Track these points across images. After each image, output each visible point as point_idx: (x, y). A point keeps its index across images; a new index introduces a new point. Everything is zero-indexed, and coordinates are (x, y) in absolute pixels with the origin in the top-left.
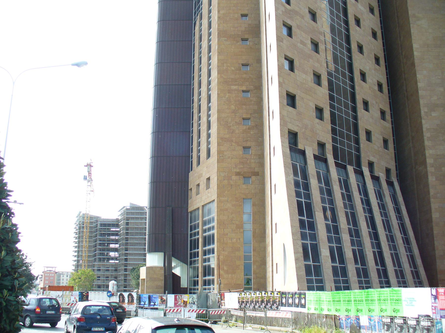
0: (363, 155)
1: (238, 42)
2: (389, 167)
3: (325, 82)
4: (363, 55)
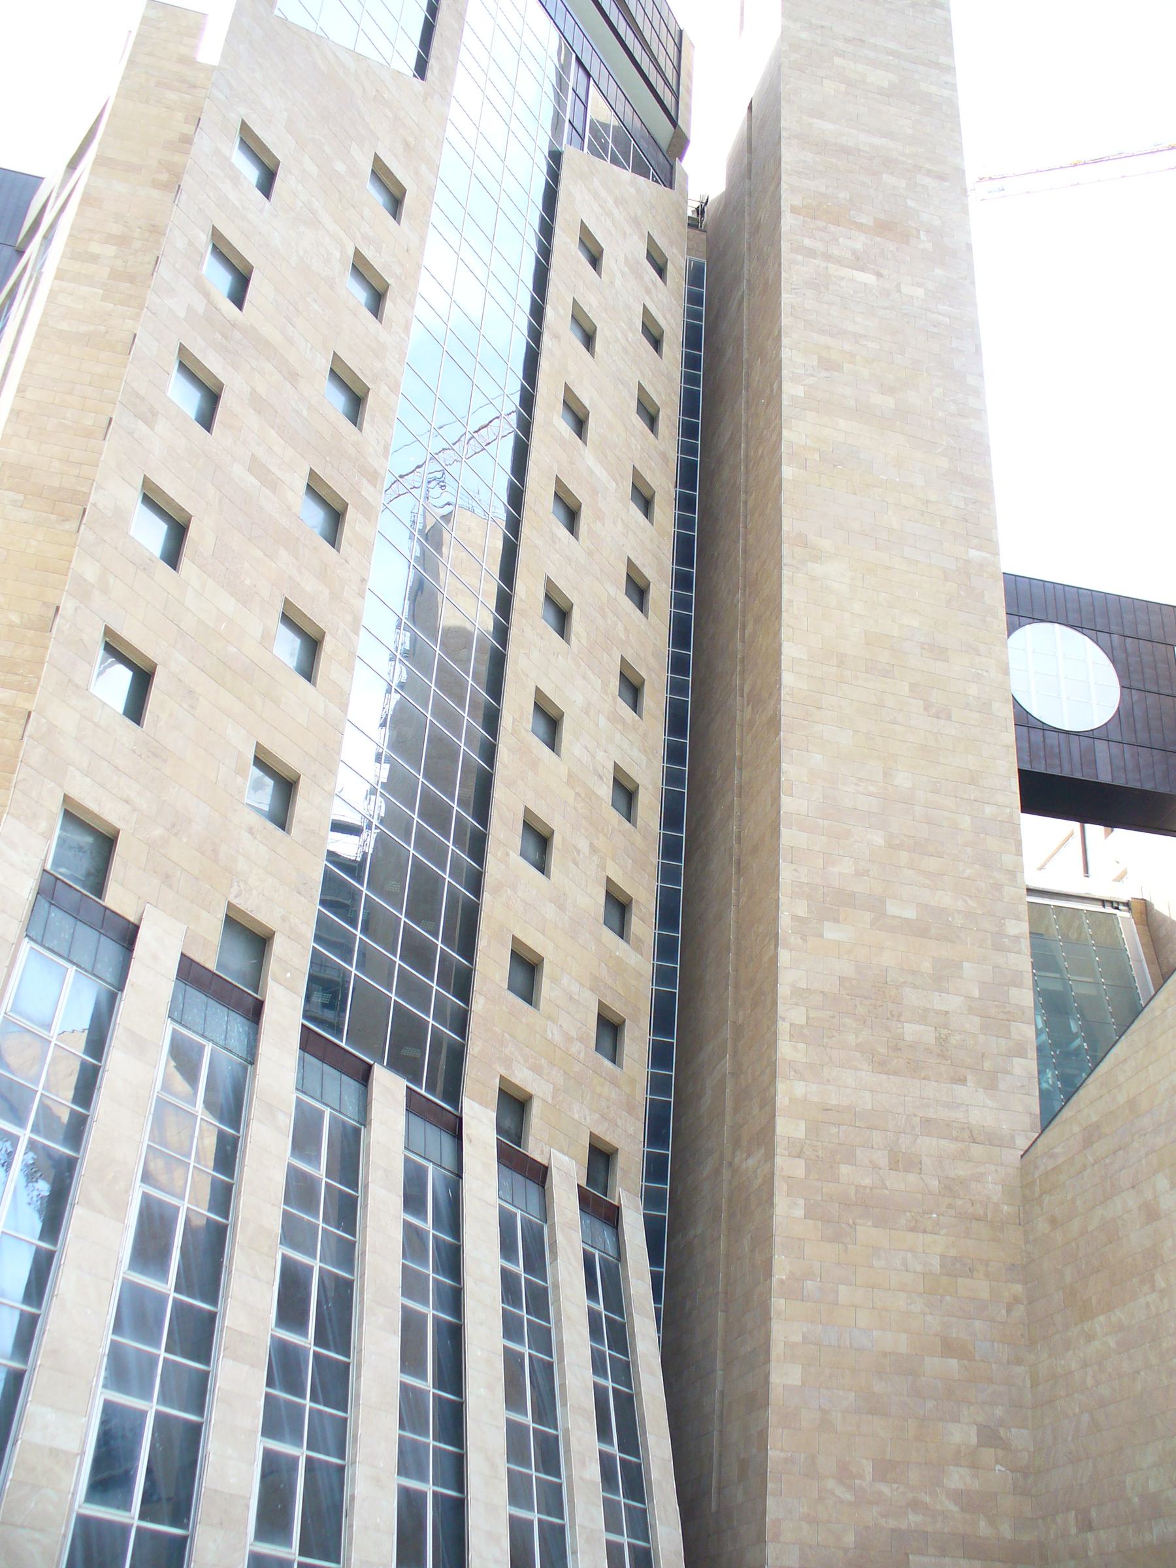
0: (474, 1048)
1: (68, 520)
2: (610, 1137)
4: (568, 642)
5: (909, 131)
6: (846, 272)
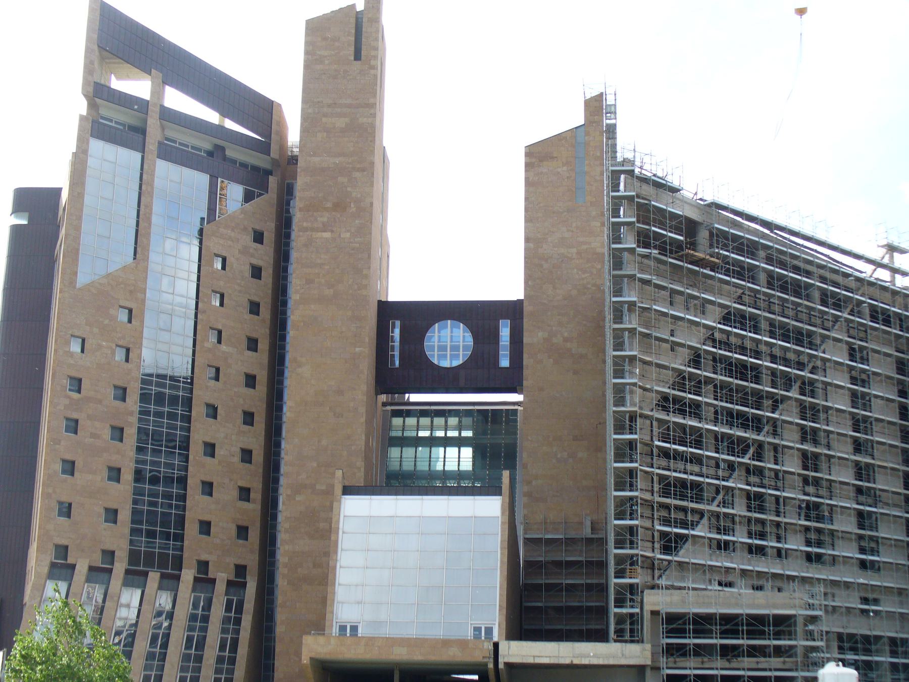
0: (185, 555)
2: (241, 562)
3: (128, 476)
5: (352, 149)
6: (319, 234)
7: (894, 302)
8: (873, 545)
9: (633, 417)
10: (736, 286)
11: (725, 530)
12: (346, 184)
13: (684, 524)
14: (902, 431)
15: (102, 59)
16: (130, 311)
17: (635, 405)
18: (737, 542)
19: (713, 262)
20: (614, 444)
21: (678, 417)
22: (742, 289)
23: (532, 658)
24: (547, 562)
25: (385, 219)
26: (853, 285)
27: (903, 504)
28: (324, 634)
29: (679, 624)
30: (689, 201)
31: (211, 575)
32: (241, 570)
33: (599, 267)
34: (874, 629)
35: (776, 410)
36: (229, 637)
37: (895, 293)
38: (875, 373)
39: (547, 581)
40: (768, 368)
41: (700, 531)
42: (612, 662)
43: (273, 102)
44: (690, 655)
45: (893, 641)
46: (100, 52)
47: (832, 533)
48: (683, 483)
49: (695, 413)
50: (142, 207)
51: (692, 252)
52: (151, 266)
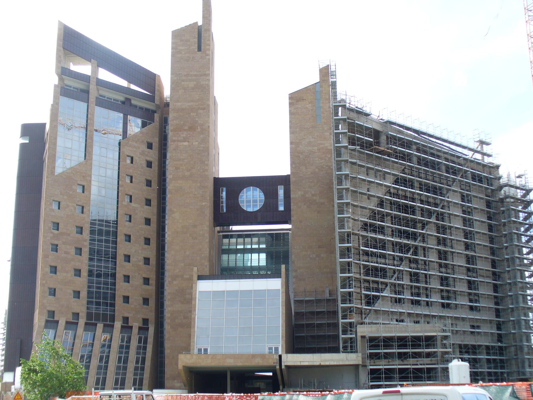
3: (85, 274)
5: (198, 98)
6: (182, 143)
7: (484, 170)
8: (476, 298)
9: (349, 235)
10: (401, 164)
11: (399, 292)
12: (195, 116)
13: (377, 290)
14: (490, 238)
15: (65, 55)
16: (84, 187)
17: (349, 228)
18: (405, 298)
19: (389, 152)
20: (339, 249)
21: (373, 234)
22: (404, 166)
23: (299, 362)
24: (306, 313)
25: (216, 134)
26: (462, 162)
27: (491, 276)
28: (190, 353)
29: (376, 342)
30: (376, 121)
31: (130, 324)
32: (146, 321)
33: (330, 156)
34: (478, 342)
35: (424, 229)
36: (141, 356)
37: (484, 166)
38: (475, 208)
39: (307, 322)
40: (419, 207)
41: (386, 293)
42: (341, 363)
43: (155, 75)
44: (382, 358)
45: (487, 347)
46: (64, 51)
47: (455, 292)
48: (376, 269)
49: (381, 232)
50: (88, 131)
51: (378, 147)
52: (94, 163)
